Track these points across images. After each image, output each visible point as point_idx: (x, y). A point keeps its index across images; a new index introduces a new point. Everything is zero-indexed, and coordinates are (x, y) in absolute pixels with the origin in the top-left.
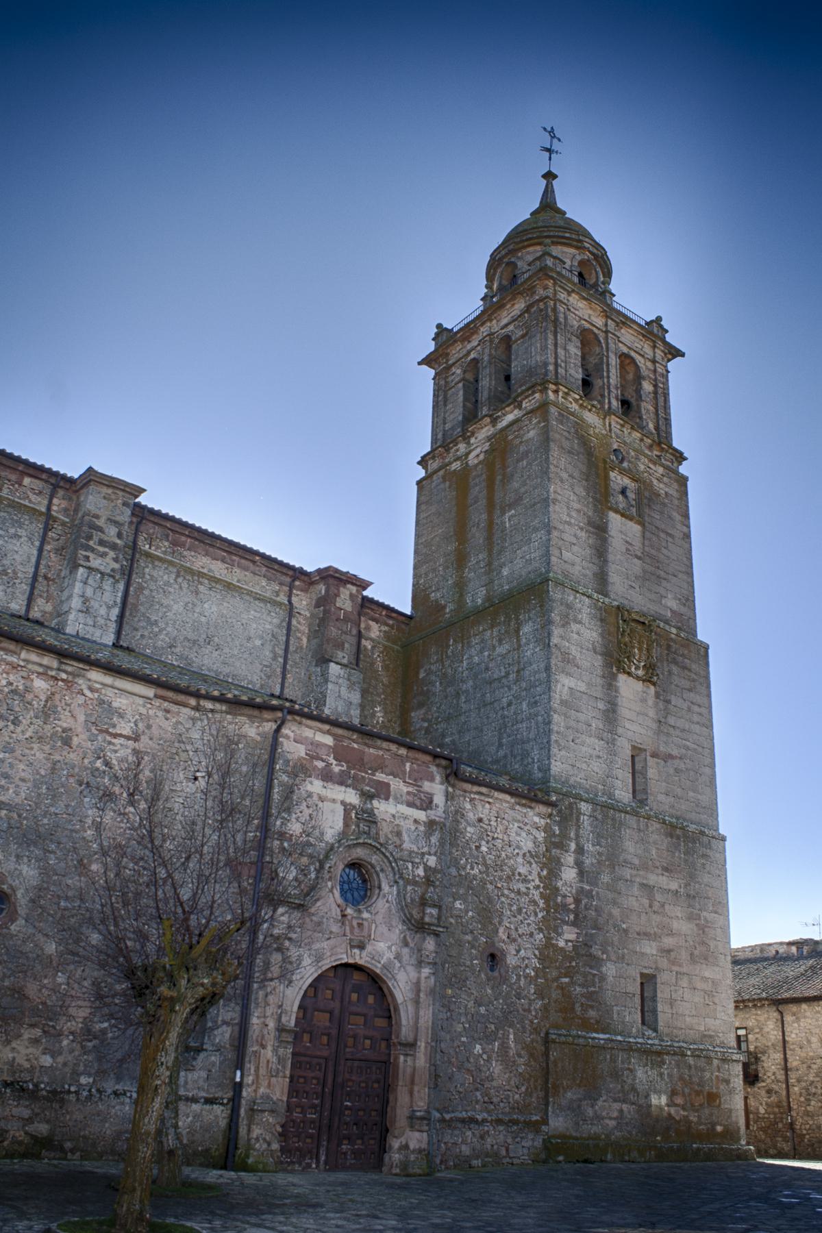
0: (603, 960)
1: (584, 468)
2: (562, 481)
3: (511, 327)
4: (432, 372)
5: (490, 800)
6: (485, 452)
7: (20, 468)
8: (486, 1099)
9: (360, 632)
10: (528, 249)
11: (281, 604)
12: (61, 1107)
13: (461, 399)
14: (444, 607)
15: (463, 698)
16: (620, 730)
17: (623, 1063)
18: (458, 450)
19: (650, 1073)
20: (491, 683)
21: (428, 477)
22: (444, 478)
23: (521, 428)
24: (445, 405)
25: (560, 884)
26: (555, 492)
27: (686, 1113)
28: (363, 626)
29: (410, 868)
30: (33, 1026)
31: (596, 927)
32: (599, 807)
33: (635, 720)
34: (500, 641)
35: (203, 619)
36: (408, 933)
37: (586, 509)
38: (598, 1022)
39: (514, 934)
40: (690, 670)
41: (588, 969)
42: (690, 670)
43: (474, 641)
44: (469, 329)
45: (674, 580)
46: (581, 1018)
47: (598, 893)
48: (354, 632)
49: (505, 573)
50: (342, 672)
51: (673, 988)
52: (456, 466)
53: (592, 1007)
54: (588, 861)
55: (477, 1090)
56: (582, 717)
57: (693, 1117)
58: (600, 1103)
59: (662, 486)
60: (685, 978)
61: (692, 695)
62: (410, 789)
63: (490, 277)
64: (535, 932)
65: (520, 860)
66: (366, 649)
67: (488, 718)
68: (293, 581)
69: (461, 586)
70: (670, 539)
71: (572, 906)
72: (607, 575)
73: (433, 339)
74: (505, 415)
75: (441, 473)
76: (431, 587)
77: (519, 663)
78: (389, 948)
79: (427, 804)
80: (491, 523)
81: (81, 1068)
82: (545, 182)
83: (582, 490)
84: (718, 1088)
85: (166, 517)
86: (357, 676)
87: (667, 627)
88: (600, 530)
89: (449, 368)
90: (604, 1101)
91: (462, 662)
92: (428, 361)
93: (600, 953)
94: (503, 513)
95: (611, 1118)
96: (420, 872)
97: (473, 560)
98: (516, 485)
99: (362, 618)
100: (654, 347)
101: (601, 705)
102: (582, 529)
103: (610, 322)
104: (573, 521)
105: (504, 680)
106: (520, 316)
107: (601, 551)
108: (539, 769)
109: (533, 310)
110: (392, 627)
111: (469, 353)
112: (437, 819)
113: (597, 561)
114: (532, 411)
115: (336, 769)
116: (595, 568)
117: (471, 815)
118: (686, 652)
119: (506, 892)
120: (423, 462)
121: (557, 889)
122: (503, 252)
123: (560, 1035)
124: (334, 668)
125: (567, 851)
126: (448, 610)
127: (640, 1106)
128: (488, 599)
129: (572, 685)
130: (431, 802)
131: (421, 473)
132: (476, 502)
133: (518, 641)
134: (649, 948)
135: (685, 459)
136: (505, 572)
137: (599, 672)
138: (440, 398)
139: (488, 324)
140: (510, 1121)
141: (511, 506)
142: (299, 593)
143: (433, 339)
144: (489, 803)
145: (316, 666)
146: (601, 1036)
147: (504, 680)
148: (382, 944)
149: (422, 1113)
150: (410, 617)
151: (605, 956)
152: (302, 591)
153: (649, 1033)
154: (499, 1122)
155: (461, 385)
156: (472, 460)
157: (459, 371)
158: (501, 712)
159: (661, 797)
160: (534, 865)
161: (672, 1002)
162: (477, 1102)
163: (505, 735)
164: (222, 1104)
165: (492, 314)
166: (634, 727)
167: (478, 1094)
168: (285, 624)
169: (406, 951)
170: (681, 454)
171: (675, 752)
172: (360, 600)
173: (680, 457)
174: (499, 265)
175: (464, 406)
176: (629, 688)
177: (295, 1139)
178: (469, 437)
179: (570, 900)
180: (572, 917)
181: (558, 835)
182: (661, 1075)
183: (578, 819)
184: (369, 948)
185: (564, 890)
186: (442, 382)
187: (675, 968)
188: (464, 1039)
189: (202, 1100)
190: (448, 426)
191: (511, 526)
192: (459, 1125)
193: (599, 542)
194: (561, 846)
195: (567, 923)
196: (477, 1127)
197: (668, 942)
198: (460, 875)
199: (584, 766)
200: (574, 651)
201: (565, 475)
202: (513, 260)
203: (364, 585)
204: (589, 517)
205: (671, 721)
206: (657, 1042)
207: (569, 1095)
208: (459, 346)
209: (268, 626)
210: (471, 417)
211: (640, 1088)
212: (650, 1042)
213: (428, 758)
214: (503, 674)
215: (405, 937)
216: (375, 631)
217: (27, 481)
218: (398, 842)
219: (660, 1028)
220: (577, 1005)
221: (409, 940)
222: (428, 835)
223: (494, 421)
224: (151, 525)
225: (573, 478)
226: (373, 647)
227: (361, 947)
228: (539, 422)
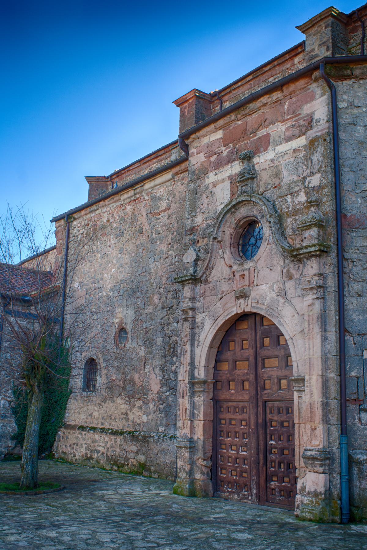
7: (288, 58)
12: (148, 446)
30: (139, 399)
36: (292, 266)
78: (271, 287)
81: (159, 422)
112: (319, 134)
115: (225, 153)
149: (313, 453)
169: (290, 285)
177: (234, 473)
184: (253, 294)
213: (301, 83)
215: (288, 271)
217: (296, 60)
221: (293, 272)
227: (243, 295)
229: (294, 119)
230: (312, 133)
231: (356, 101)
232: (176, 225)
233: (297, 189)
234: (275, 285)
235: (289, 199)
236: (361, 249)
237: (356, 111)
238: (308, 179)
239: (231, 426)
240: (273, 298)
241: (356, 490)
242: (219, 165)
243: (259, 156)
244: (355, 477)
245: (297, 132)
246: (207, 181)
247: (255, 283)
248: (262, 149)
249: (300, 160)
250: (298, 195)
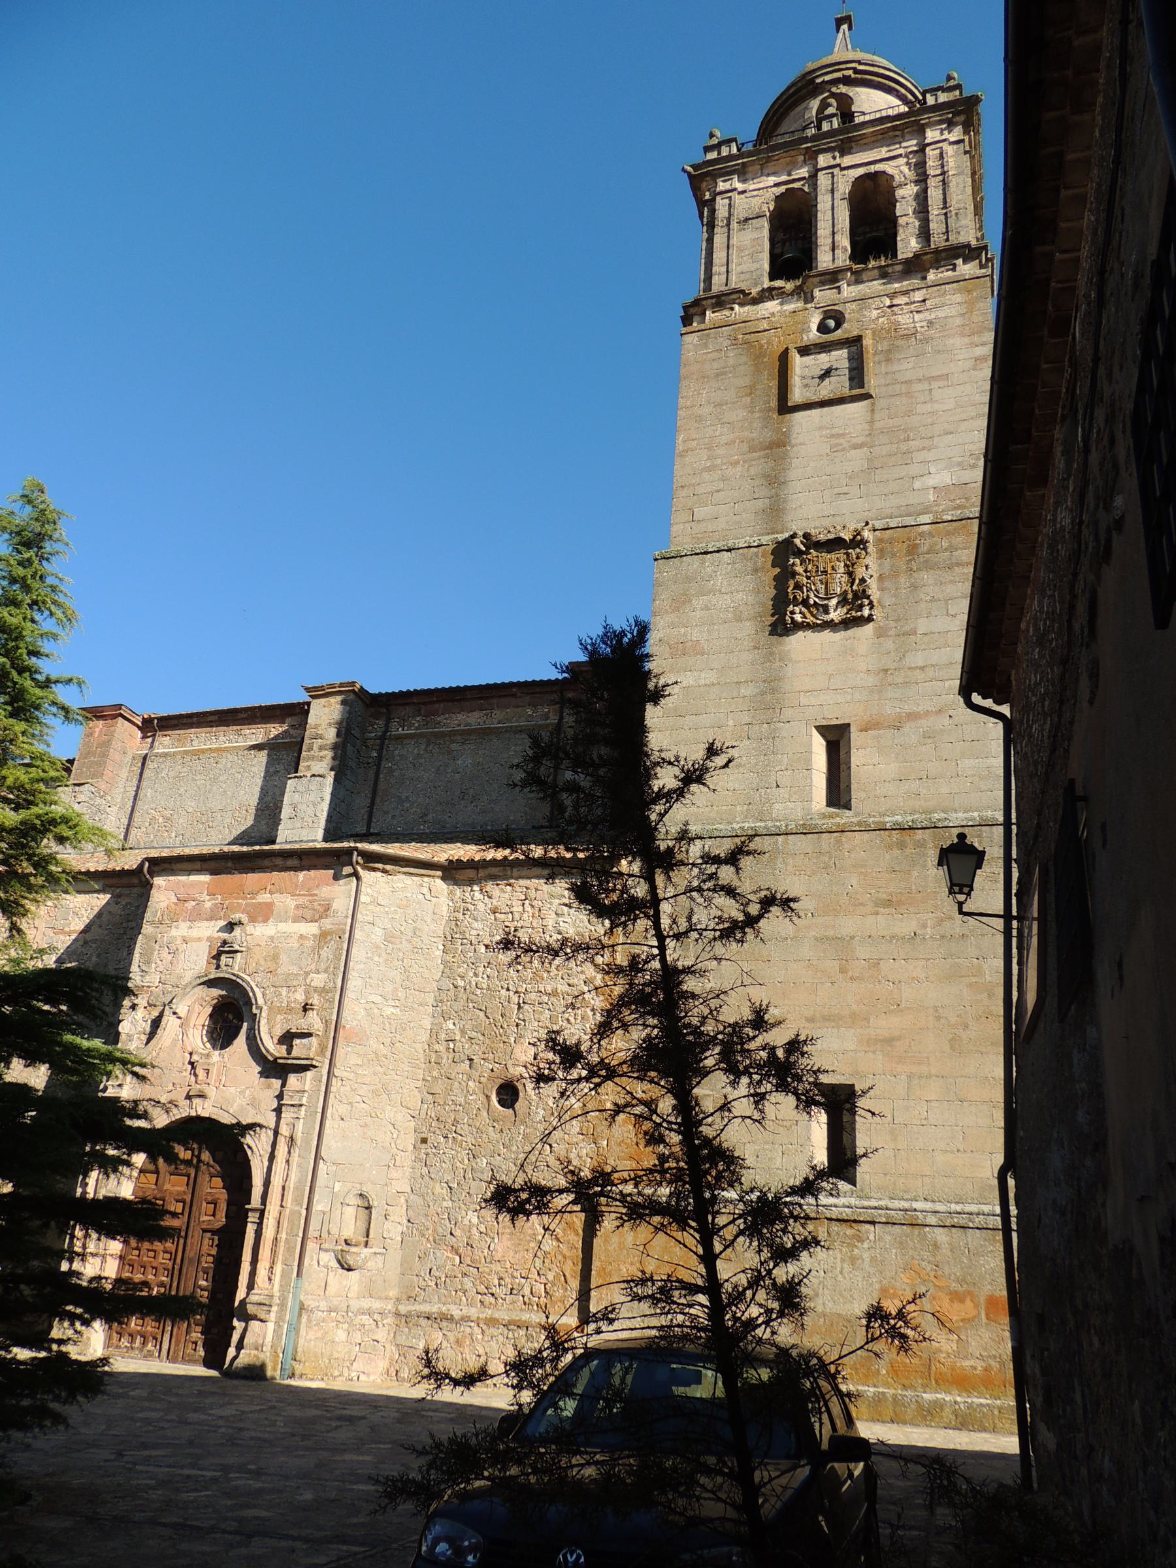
8: (482, 1289)
35: (457, 776)
62: (301, 900)
115: (208, 905)
117: (481, 906)
140: (511, 1322)
144: (510, 885)
148: (232, 1090)
154: (492, 1322)
192: (424, 1322)
197: (884, 1025)
198: (456, 987)
229: (307, 898)
230: (327, 924)
231: (380, 898)
232: (94, 959)
233: (295, 983)
234: (248, 1091)
235: (284, 991)
236: (353, 1068)
237: (378, 909)
238: (312, 975)
240: (242, 1106)
241: (301, 1342)
242: (196, 916)
243: (255, 927)
244: (303, 1326)
245: (308, 914)
246: (174, 932)
247: (223, 1082)
248: (260, 919)
249: (306, 950)
250: (296, 991)
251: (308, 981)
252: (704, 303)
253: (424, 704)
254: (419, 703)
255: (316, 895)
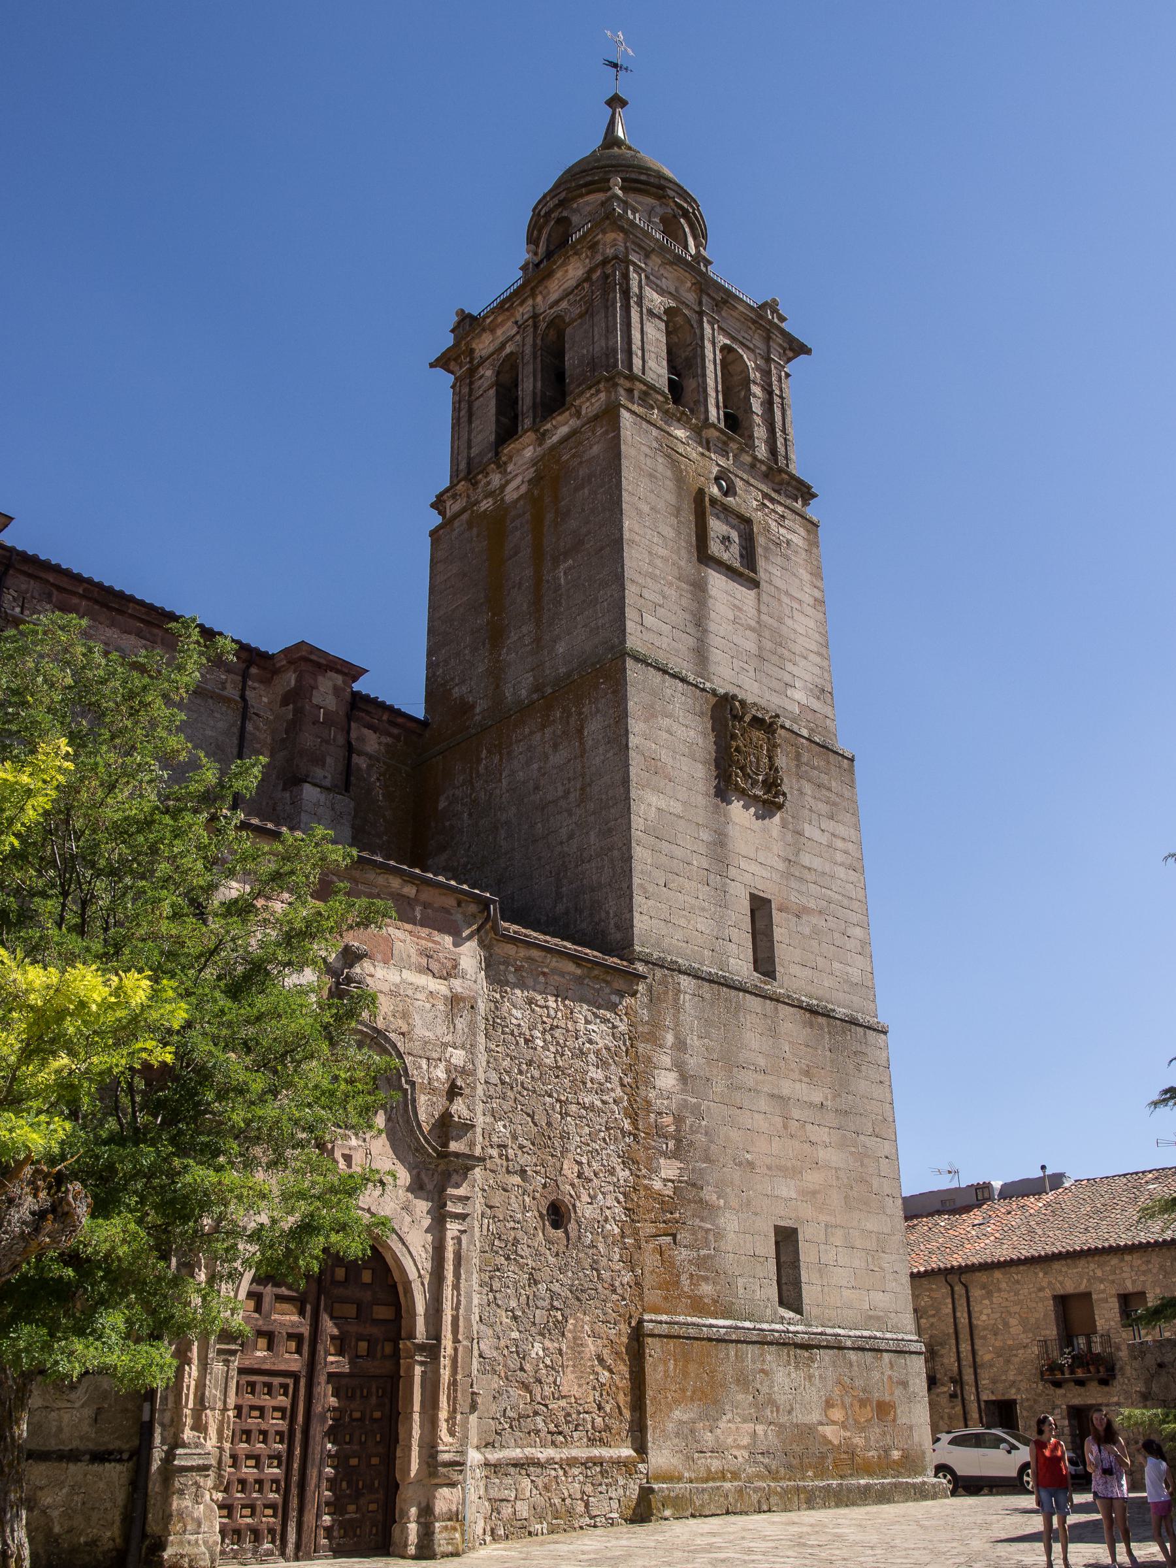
0: (719, 1208)
1: (672, 498)
2: (640, 513)
3: (564, 304)
4: (451, 378)
5: (546, 970)
6: (530, 481)
8: (552, 1427)
9: (349, 743)
10: (586, 199)
11: (227, 700)
13: (493, 410)
14: (473, 707)
15: (503, 833)
16: (733, 872)
17: (754, 1362)
18: (489, 483)
19: (793, 1375)
20: (543, 809)
21: (447, 523)
22: (470, 524)
23: (581, 443)
24: (470, 422)
25: (652, 1095)
26: (630, 530)
27: (848, 1434)
28: (353, 735)
29: (425, 1067)
31: (707, 1159)
32: (706, 984)
33: (752, 855)
34: (555, 746)
37: (675, 557)
38: (715, 1302)
39: (588, 1173)
40: (829, 789)
41: (697, 1221)
42: (829, 789)
43: (518, 749)
44: (505, 306)
45: (803, 663)
46: (689, 1297)
47: (708, 1108)
48: (341, 740)
49: (561, 650)
50: (322, 798)
51: (822, 1247)
52: (486, 505)
53: (706, 1279)
54: (693, 1062)
55: (536, 1413)
56: (678, 852)
57: (858, 1441)
58: (722, 1424)
59: (782, 531)
60: (839, 1233)
61: (832, 823)
63: (532, 240)
64: (618, 1168)
65: (592, 1057)
66: (359, 769)
67: (539, 859)
68: (248, 667)
69: (496, 674)
70: (796, 605)
71: (672, 1128)
72: (708, 651)
73: (452, 331)
74: (556, 428)
75: (465, 516)
76: (452, 679)
77: (583, 775)
79: (450, 972)
80: (538, 581)
82: (610, 111)
83: (670, 529)
84: (892, 1394)
85: (47, 566)
86: (344, 803)
87: (795, 728)
88: (699, 588)
89: (472, 371)
90: (729, 1421)
91: (500, 781)
92: (443, 362)
93: (714, 1197)
94: (556, 562)
95: (739, 1447)
96: (440, 1073)
97: (514, 636)
98: (573, 524)
99: (353, 725)
100: (768, 339)
101: (705, 835)
102: (671, 584)
103: (705, 299)
104: (658, 572)
105: (563, 803)
106: (576, 287)
107: (699, 620)
108: (617, 927)
109: (595, 277)
110: (397, 738)
111: (503, 346)
113: (691, 629)
114: (596, 418)
116: (691, 642)
118: (822, 763)
119: (573, 1108)
120: (438, 504)
121: (648, 1103)
122: (551, 204)
123: (661, 1322)
124: (310, 793)
125: (661, 1046)
126: (478, 710)
127: (781, 1426)
128: (537, 688)
129: (662, 804)
130: (455, 967)
131: (437, 520)
132: (516, 554)
133: (582, 743)
134: (786, 1189)
135: (814, 496)
136: (561, 648)
137: (701, 786)
138: (462, 413)
139: (530, 302)
141: (566, 554)
142: (256, 685)
143: (452, 331)
145: (284, 789)
146: (721, 1322)
147: (563, 803)
150: (424, 724)
151: (722, 1202)
152: (261, 682)
153: (789, 1314)
155: (492, 392)
156: (511, 494)
157: (489, 373)
158: (559, 849)
159: (795, 970)
160: (613, 1067)
161: (822, 1268)
162: (537, 1432)
163: (565, 881)
164: (120, 1461)
165: (536, 286)
166: (753, 868)
167: (539, 1419)
168: (235, 730)
170: (809, 487)
171: (812, 904)
172: (348, 696)
173: (804, 492)
174: (546, 222)
175: (498, 421)
176: (739, 813)
178: (505, 463)
179: (667, 1120)
180: (671, 1144)
181: (647, 1023)
182: (810, 1377)
183: (676, 1000)
185: (659, 1104)
186: (465, 390)
187: (823, 1218)
188: (515, 1335)
189: (87, 1457)
190: (474, 451)
191: (567, 583)
192: (512, 1470)
193: (696, 604)
194: (653, 1039)
195: (664, 1154)
196: (539, 1470)
197: (813, 1179)
199: (683, 922)
200: (665, 756)
201: (646, 508)
202: (565, 214)
203: (353, 672)
204: (679, 568)
205: (806, 859)
206: (800, 1328)
207: (677, 1414)
208: (487, 338)
209: (209, 733)
210: (507, 432)
211: (781, 1399)
212: (792, 1328)
214: (560, 793)
216: (372, 742)
218: (405, 1029)
219: (806, 1308)
220: (684, 1277)
221: (426, 1180)
222: (451, 1017)
223: (542, 438)
224: (23, 578)
225: (657, 512)
226: (370, 767)
228: (606, 432)
235: (424, 1063)
238: (450, 1049)
239: (249, 1420)
243: (375, 966)
251: (448, 1055)
252: (637, 383)
253: (60, 589)
254: (53, 585)
255: (439, 943)
